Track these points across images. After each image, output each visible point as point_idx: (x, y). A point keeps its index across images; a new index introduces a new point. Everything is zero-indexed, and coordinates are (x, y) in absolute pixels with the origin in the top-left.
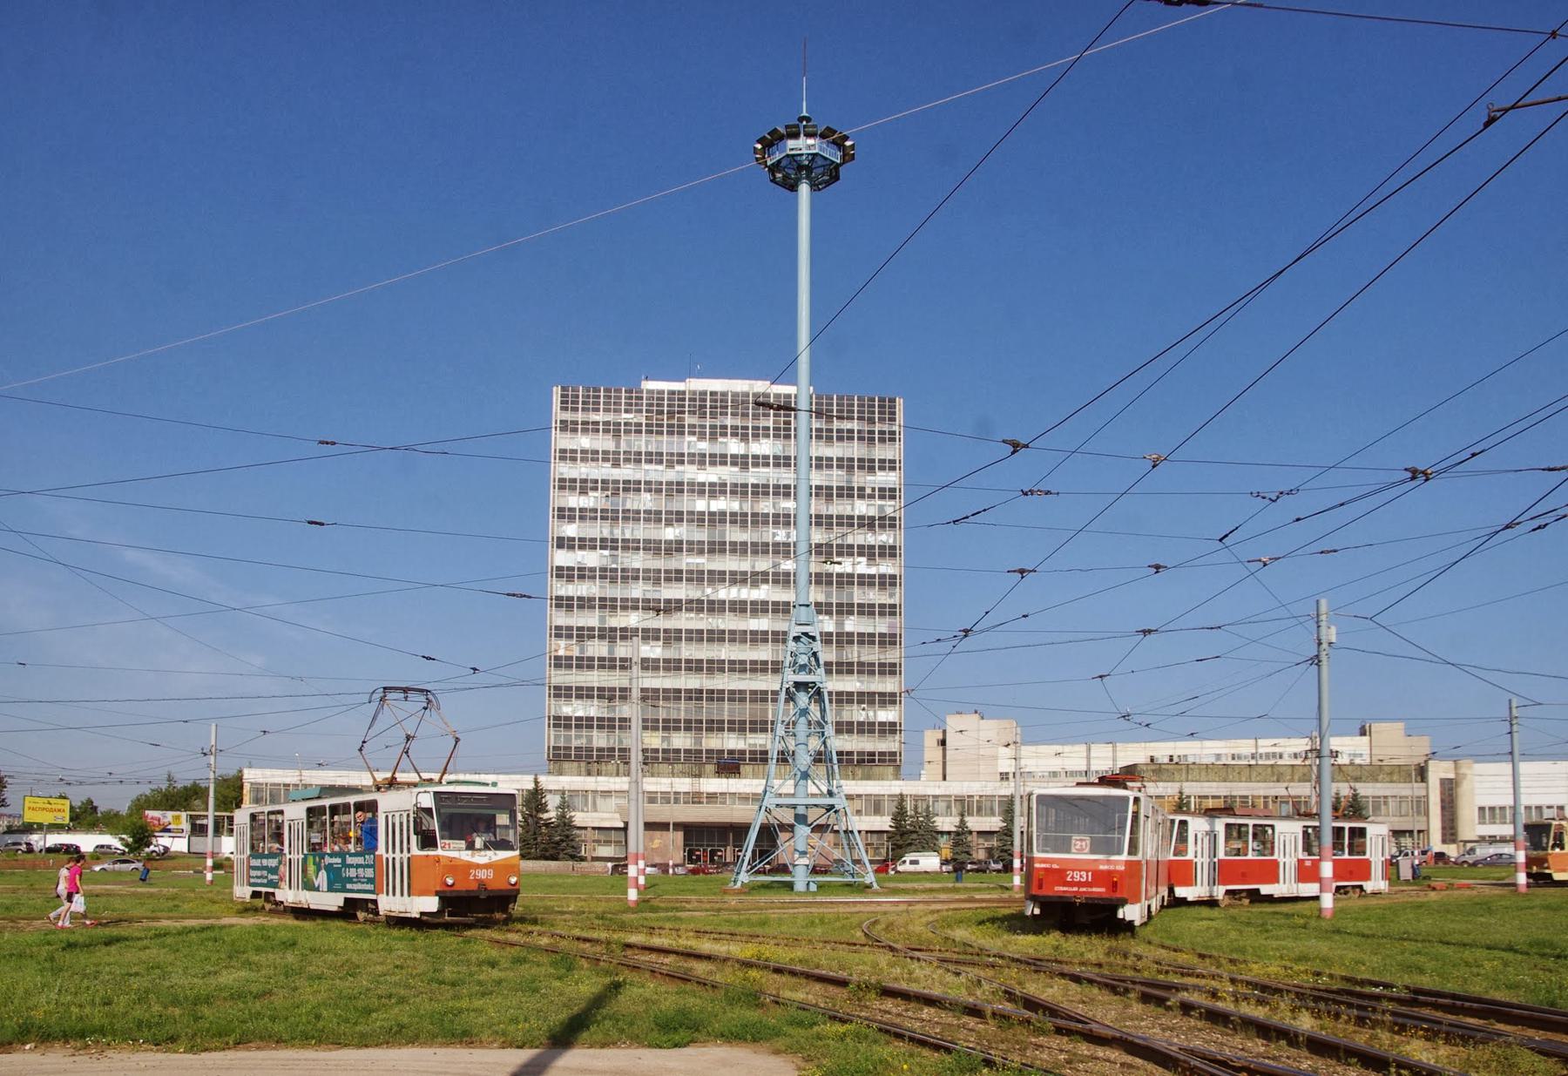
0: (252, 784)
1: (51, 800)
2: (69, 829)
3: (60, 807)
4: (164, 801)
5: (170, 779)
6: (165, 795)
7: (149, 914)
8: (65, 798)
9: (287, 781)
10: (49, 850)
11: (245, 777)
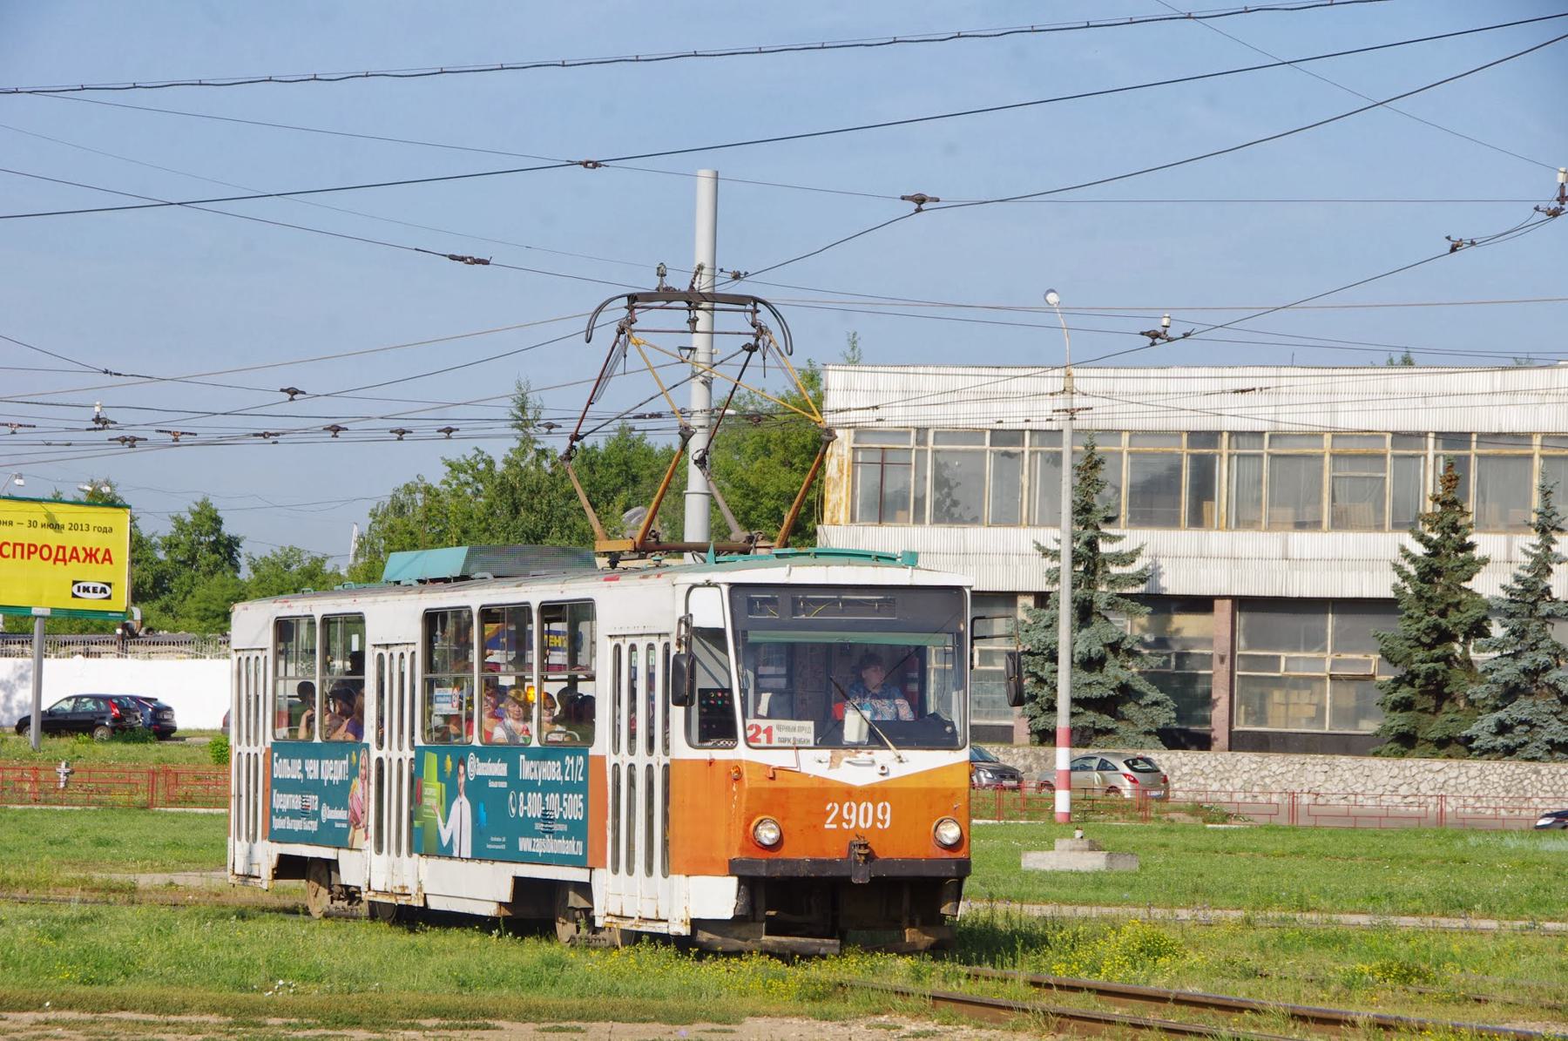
0: (860, 431)
1: (63, 514)
2: (130, 635)
3: (92, 540)
4: (503, 511)
5: (524, 417)
6: (505, 488)
7: (448, 996)
8: (112, 503)
9: (1013, 416)
10: (56, 724)
11: (832, 402)
